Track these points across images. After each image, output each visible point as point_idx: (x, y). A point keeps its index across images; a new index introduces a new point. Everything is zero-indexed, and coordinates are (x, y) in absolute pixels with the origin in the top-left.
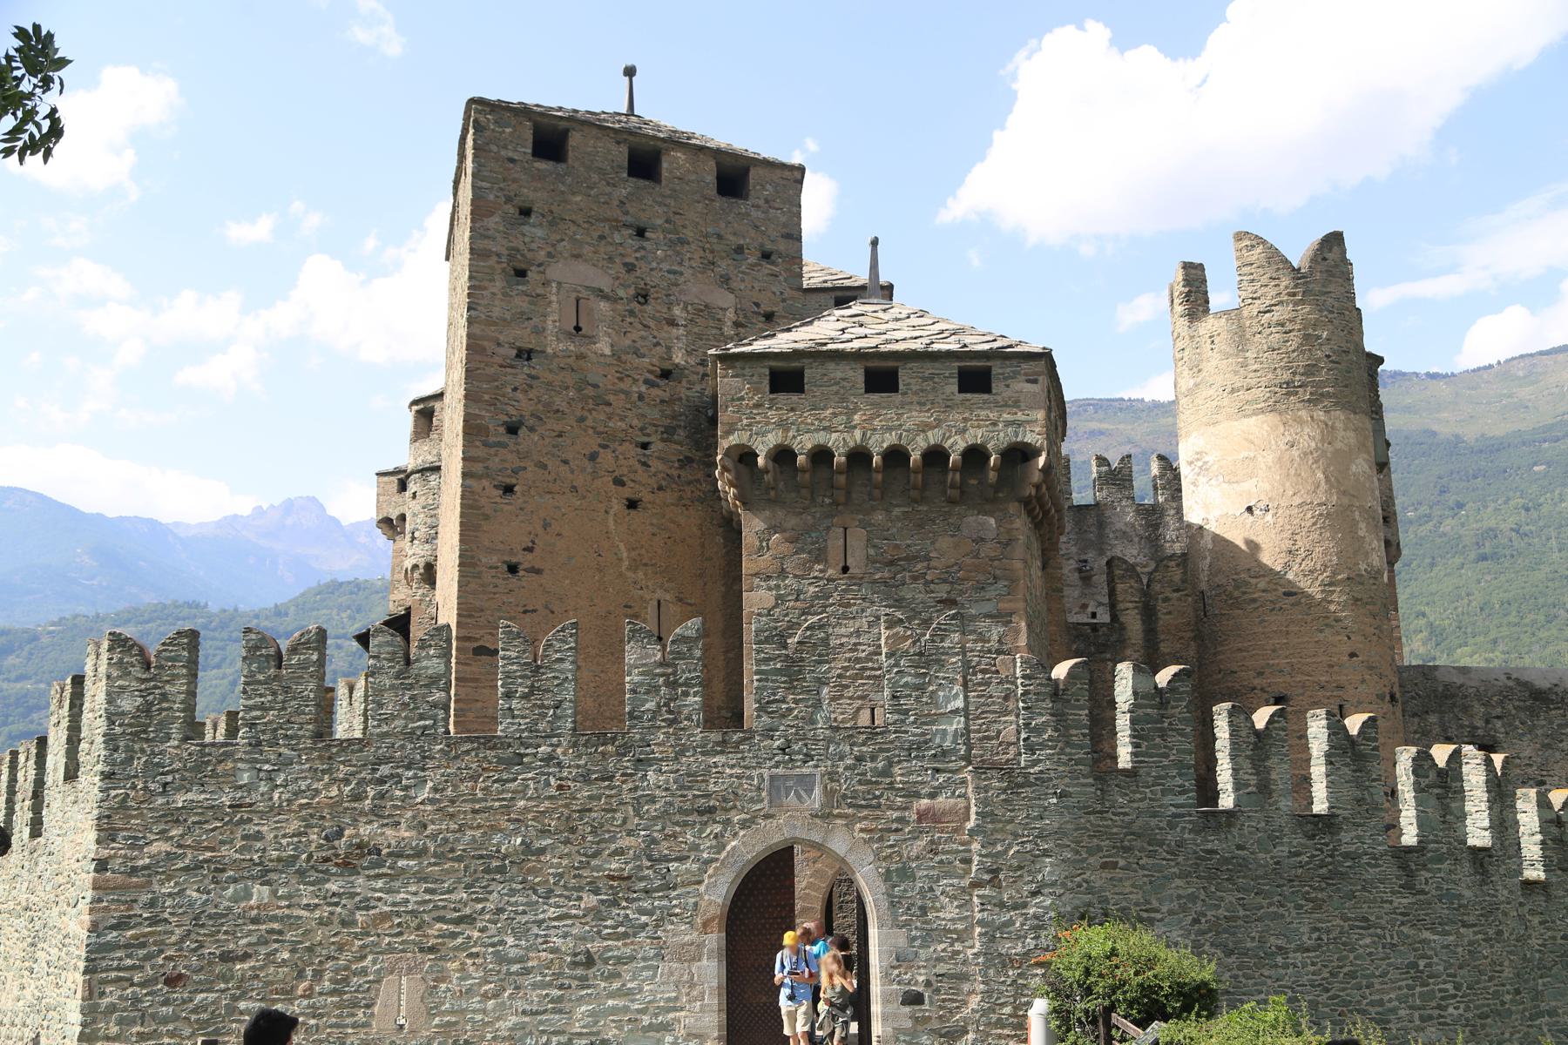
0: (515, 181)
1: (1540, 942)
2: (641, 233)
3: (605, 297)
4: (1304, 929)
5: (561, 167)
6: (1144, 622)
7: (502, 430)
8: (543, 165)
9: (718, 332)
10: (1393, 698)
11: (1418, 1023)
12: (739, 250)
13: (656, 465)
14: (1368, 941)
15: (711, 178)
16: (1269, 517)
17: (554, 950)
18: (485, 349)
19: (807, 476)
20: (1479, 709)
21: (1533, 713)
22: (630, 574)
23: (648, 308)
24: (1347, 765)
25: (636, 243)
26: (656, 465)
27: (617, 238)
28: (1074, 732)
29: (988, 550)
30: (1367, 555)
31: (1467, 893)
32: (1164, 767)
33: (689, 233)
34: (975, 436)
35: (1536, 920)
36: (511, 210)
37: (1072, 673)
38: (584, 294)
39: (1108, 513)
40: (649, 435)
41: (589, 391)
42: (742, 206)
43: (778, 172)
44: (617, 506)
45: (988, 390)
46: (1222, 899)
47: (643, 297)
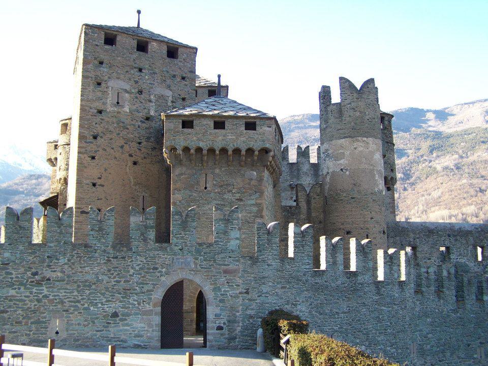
0: (98, 52)
1: (419, 309)
2: (140, 70)
3: (128, 92)
4: (345, 307)
6: (307, 206)
7: (91, 137)
8: (107, 47)
9: (166, 104)
10: (384, 232)
11: (378, 334)
12: (174, 76)
13: (143, 150)
14: (364, 310)
15: (165, 52)
16: (348, 173)
17: (106, 312)
18: (86, 110)
19: (194, 156)
20: (412, 235)
21: (428, 236)
22: (134, 187)
23: (142, 96)
24: (361, 256)
25: (139, 74)
26: (143, 150)
27: (132, 72)
28: (274, 245)
29: (253, 183)
30: (378, 185)
31: (397, 295)
32: (303, 257)
34: (251, 144)
35: (418, 303)
36: (96, 62)
37: (274, 227)
38: (120, 91)
39: (301, 166)
40: (141, 140)
41: (121, 124)
43: (188, 49)
44: (130, 164)
45: (255, 129)
46: (319, 297)
47: (140, 92)
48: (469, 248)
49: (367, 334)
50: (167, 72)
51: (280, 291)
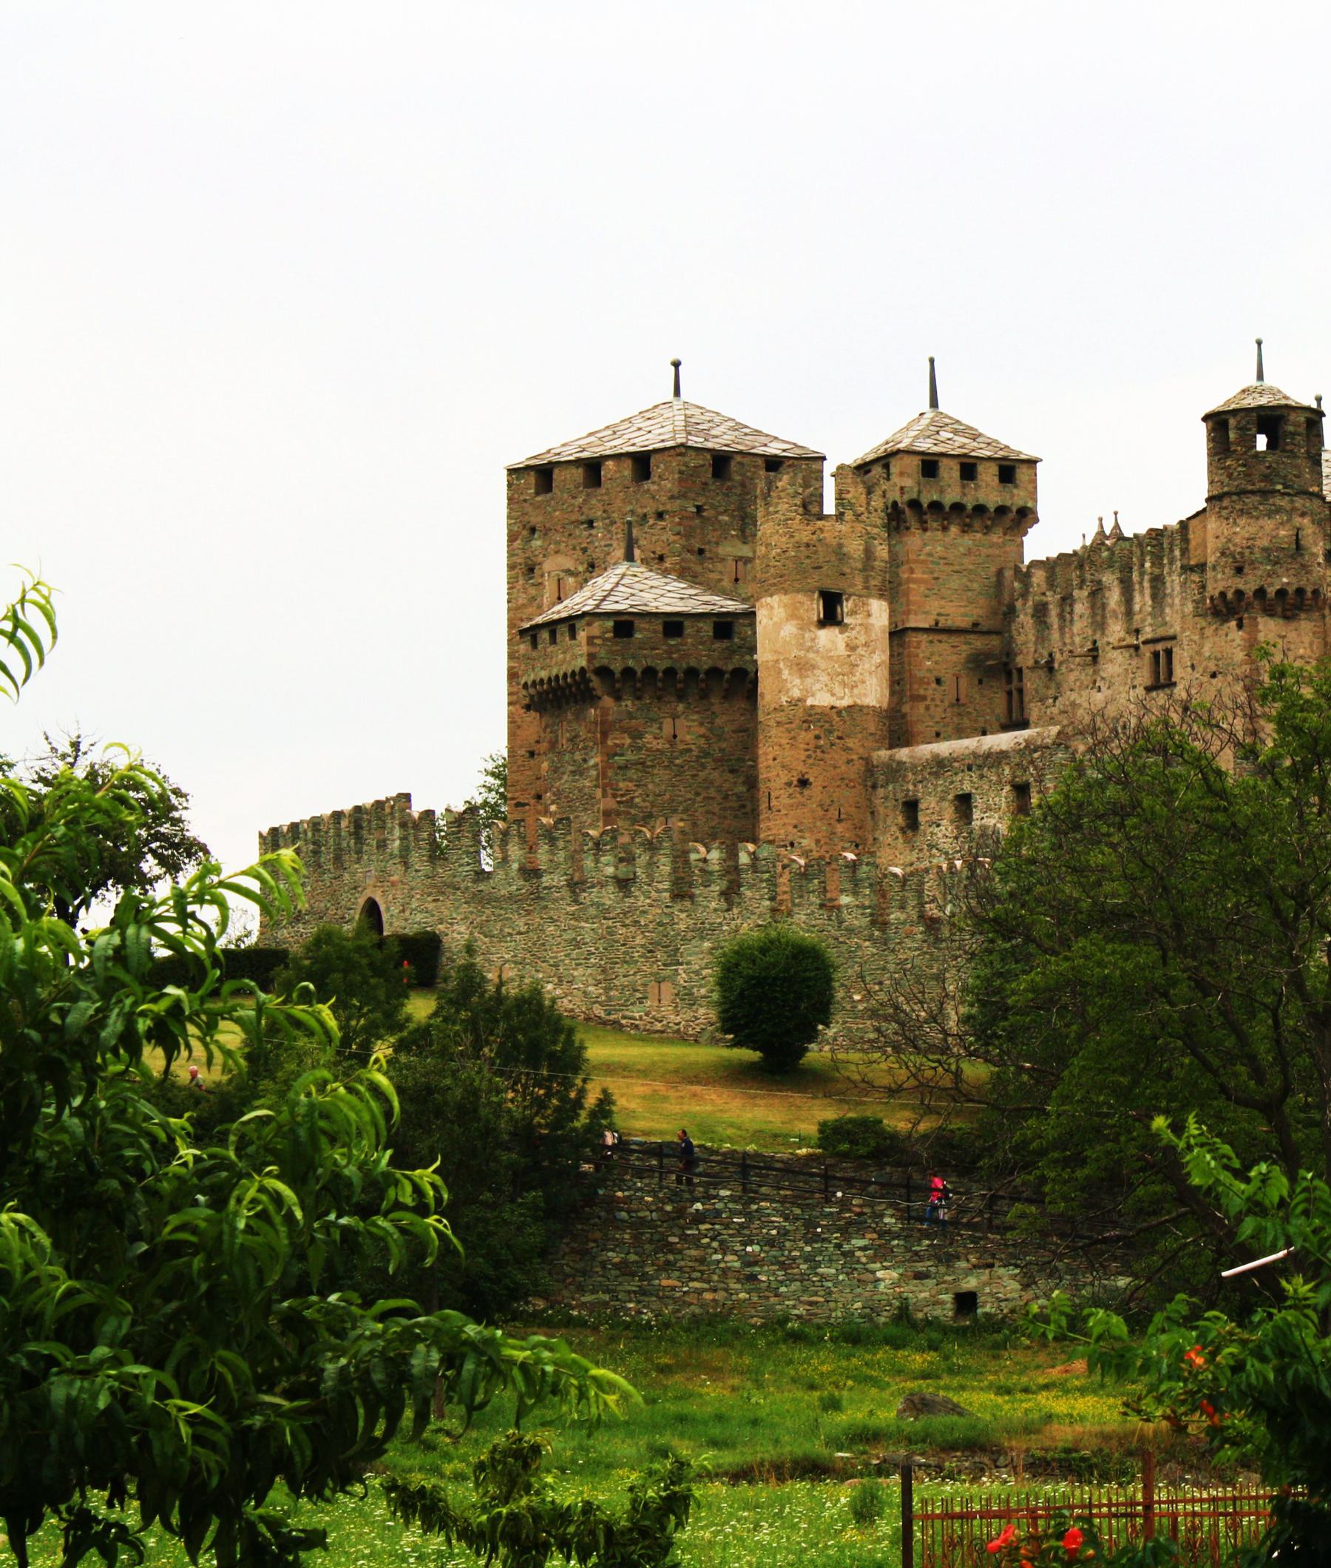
2: (590, 524)
5: (549, 495)
8: (539, 499)
12: (645, 515)
21: (937, 775)
27: (577, 532)
30: (788, 691)
33: (615, 515)
35: (683, 915)
36: (525, 533)
42: (647, 485)
48: (1004, 793)
49: (556, 966)
50: (632, 512)
51: (431, 906)
